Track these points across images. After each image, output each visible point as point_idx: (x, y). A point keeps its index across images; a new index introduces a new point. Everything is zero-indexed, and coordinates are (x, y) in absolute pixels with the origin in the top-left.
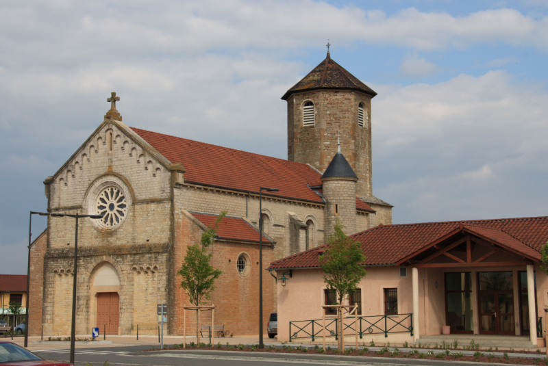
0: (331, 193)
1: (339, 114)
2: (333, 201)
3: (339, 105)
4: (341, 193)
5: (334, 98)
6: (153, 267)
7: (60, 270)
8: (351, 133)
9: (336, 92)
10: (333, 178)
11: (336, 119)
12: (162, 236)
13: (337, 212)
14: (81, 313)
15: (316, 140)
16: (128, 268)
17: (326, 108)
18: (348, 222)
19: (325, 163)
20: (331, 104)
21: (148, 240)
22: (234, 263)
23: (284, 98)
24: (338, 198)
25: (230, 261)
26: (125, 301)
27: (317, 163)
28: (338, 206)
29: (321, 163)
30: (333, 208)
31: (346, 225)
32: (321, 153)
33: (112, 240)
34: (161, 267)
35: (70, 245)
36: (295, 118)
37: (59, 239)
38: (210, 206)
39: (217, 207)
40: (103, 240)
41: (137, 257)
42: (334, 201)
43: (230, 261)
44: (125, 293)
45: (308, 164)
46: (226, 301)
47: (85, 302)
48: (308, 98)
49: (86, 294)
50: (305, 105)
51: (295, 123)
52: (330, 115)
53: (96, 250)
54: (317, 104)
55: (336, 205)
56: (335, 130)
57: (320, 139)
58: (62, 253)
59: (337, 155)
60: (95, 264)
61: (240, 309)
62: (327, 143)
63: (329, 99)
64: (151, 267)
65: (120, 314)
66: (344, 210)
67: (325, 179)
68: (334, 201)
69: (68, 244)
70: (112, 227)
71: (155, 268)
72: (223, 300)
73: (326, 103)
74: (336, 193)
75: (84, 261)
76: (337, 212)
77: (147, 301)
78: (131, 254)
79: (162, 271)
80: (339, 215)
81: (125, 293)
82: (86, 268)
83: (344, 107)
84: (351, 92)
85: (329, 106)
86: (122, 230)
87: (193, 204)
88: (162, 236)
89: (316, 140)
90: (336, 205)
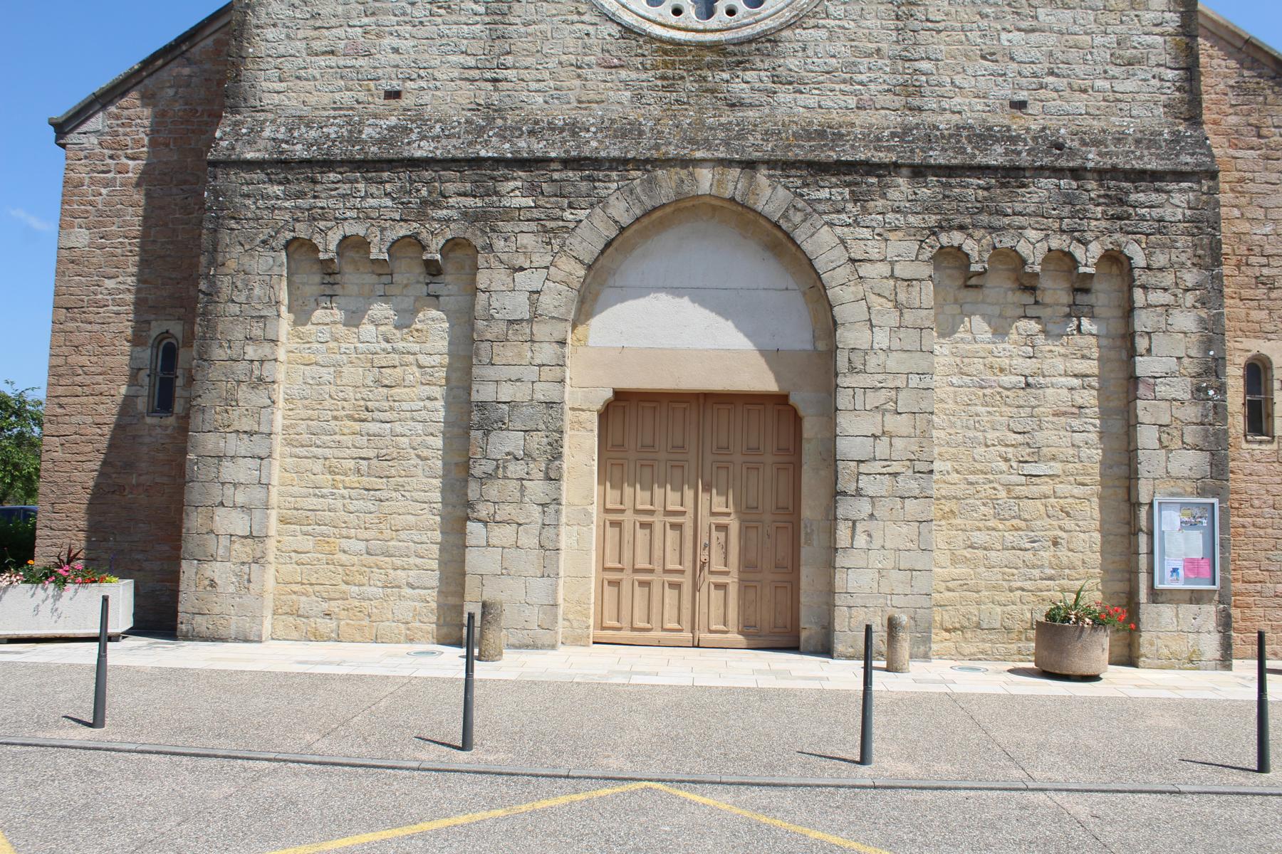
6: (1096, 249)
7: (334, 238)
12: (1130, 85)
14: (505, 512)
16: (902, 246)
21: (1020, 105)
26: (882, 448)
33: (741, 85)
34: (1160, 259)
35: (407, 101)
37: (322, 61)
40: (669, 84)
41: (972, 189)
44: (873, 399)
47: (538, 441)
49: (544, 391)
53: (630, 131)
58: (353, 141)
60: (621, 210)
64: (1079, 252)
65: (843, 532)
69: (394, 95)
70: (712, 23)
71: (1115, 260)
75: (533, 189)
77: (1037, 455)
78: (919, 172)
79: (1168, 279)
81: (873, 399)
82: (552, 231)
86: (823, 33)
88: (1130, 85)
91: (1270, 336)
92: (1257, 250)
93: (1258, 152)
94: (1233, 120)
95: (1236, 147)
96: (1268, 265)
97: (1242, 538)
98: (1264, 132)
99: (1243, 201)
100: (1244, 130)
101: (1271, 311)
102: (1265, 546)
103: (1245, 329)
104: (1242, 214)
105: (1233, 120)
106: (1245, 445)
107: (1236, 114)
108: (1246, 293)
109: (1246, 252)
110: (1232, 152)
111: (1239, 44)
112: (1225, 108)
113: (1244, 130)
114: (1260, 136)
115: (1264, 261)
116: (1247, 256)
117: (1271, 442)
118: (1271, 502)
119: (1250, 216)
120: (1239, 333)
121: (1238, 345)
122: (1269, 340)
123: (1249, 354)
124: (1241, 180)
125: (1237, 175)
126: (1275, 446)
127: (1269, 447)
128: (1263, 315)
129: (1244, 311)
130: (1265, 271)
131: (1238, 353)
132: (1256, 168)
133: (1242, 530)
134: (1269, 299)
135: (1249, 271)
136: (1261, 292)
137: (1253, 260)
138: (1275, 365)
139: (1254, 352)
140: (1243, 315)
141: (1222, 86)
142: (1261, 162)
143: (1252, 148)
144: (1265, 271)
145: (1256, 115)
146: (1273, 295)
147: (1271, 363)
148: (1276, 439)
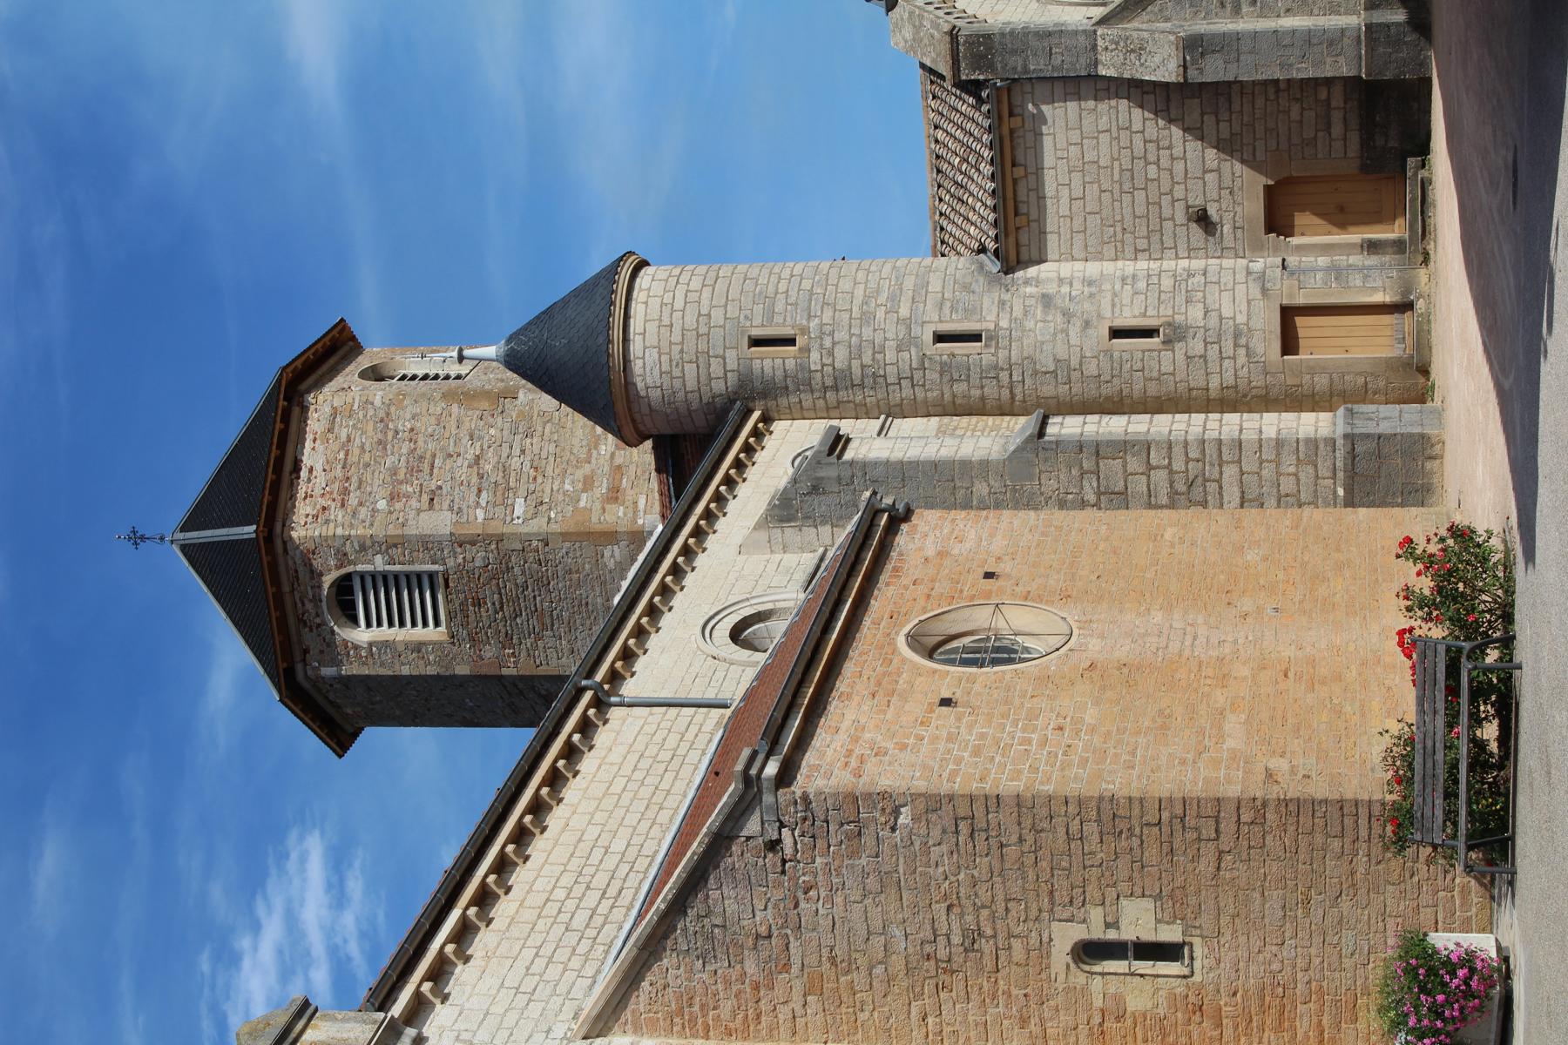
0: (690, 370)
1: (397, 457)
2: (732, 365)
3: (353, 458)
4: (690, 320)
5: (320, 480)
8: (485, 405)
9: (297, 468)
10: (616, 348)
11: (412, 471)
13: (791, 341)
15: (504, 558)
17: (363, 512)
18: (846, 285)
19: (609, 518)
20: (345, 492)
22: (972, 680)
23: (339, 737)
24: (717, 334)
25: (946, 702)
27: (612, 554)
28: (757, 332)
29: (611, 537)
30: (770, 362)
31: (859, 292)
32: (565, 536)
36: (405, 671)
38: (600, 880)
39: (618, 845)
42: (731, 356)
43: (946, 702)
45: (616, 600)
46: (1234, 725)
48: (317, 599)
50: (354, 620)
51: (431, 671)
52: (393, 498)
54: (343, 559)
55: (757, 342)
56: (462, 471)
57: (500, 539)
59: (513, 362)
61: (1290, 652)
62: (520, 508)
63: (322, 502)
66: (779, 307)
67: (620, 407)
68: (731, 356)
72: (1221, 737)
73: (337, 514)
74: (690, 346)
76: (791, 341)
80: (805, 331)
83: (370, 435)
84: (304, 409)
85: (353, 500)
87: (553, 972)
89: (504, 558)
90: (757, 342)
91: (1046, 939)
92: (928, 949)
93: (792, 939)
94: (751, 967)
95: (786, 967)
96: (948, 936)
97: (1325, 984)
98: (763, 930)
99: (862, 961)
100: (764, 954)
101: (1010, 936)
102: (1335, 958)
103: (1038, 969)
104: (880, 963)
105: (751, 967)
106: (1197, 978)
107: (742, 962)
108: (988, 962)
109: (932, 962)
110: (795, 969)
111: (645, 955)
112: (734, 974)
113: (764, 954)
114: (770, 936)
115: (942, 941)
116: (937, 961)
117: (1191, 945)
118: (1274, 949)
119: (881, 955)
120: (1044, 976)
121: (1061, 978)
122: (1051, 940)
123: (1072, 966)
124: (833, 961)
125: (826, 965)
126: (1197, 941)
127: (1198, 952)
128: (1017, 944)
129: (1014, 968)
130: (956, 940)
131: (1071, 978)
132: (815, 943)
133: (1314, 984)
134: (994, 936)
135: (958, 959)
136: (986, 946)
137: (942, 953)
138: (1085, 936)
139: (1069, 959)
140: (1020, 970)
141: (705, 976)
142: (807, 935)
143: (787, 946)
144: (956, 940)
145: (741, 939)
146: (989, 932)
147: (1082, 941)
148: (1187, 939)
